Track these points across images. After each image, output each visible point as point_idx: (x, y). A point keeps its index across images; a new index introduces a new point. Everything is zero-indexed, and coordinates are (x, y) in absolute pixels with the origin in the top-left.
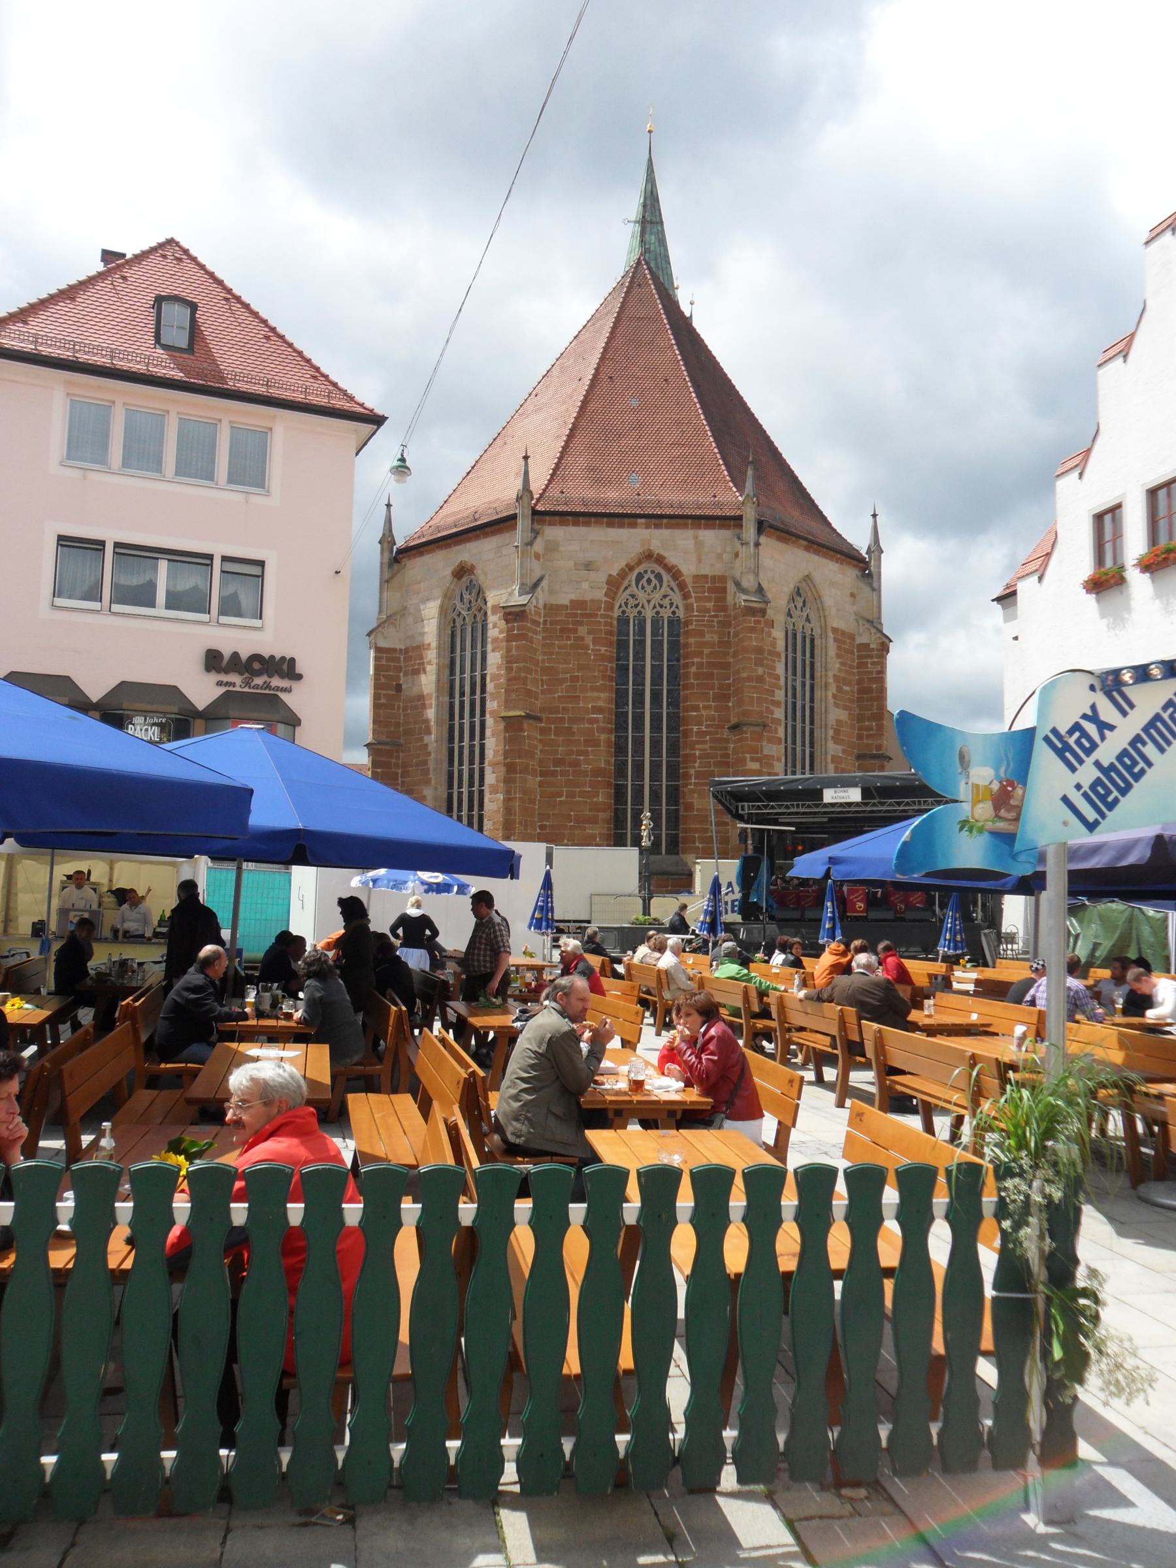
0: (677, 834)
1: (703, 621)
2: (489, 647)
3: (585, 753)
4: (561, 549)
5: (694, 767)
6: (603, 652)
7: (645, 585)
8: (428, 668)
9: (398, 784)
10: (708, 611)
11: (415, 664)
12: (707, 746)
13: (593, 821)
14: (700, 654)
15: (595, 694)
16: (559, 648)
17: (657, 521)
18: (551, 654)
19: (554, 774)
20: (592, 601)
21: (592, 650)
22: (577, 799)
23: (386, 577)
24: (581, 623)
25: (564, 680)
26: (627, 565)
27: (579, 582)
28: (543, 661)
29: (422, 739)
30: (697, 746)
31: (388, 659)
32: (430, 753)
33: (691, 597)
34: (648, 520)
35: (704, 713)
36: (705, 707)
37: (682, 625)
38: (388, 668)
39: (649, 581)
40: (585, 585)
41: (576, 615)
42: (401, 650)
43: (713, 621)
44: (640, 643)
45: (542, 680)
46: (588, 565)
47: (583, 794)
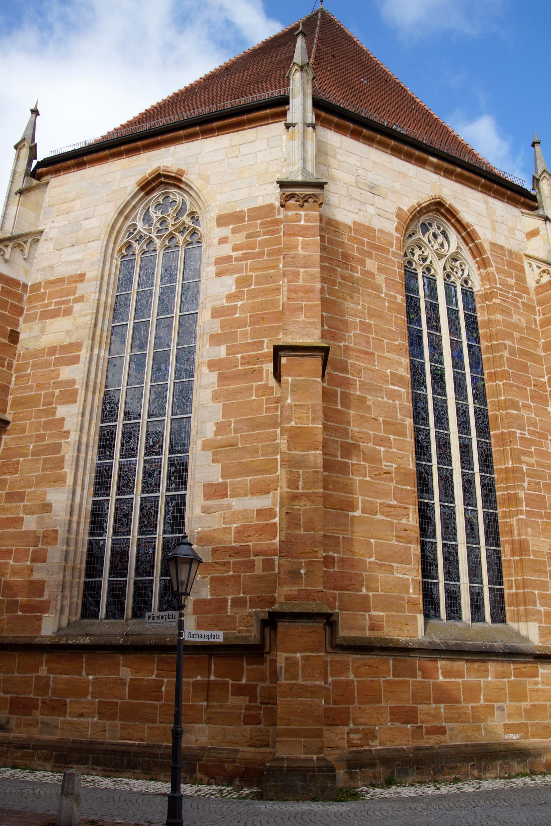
0: (502, 590)
1: (508, 298)
5: (524, 489)
7: (431, 237)
8: (77, 307)
10: (510, 287)
12: (533, 460)
14: (510, 337)
16: (343, 277)
17: (451, 167)
20: (380, 231)
21: (386, 295)
22: (379, 517)
23: (19, 185)
24: (370, 256)
29: (53, 412)
30: (524, 458)
32: (68, 432)
33: (491, 265)
34: (441, 162)
36: (525, 406)
37: (477, 299)
39: (435, 236)
41: (362, 243)
44: (433, 308)
46: (373, 187)
47: (387, 509)
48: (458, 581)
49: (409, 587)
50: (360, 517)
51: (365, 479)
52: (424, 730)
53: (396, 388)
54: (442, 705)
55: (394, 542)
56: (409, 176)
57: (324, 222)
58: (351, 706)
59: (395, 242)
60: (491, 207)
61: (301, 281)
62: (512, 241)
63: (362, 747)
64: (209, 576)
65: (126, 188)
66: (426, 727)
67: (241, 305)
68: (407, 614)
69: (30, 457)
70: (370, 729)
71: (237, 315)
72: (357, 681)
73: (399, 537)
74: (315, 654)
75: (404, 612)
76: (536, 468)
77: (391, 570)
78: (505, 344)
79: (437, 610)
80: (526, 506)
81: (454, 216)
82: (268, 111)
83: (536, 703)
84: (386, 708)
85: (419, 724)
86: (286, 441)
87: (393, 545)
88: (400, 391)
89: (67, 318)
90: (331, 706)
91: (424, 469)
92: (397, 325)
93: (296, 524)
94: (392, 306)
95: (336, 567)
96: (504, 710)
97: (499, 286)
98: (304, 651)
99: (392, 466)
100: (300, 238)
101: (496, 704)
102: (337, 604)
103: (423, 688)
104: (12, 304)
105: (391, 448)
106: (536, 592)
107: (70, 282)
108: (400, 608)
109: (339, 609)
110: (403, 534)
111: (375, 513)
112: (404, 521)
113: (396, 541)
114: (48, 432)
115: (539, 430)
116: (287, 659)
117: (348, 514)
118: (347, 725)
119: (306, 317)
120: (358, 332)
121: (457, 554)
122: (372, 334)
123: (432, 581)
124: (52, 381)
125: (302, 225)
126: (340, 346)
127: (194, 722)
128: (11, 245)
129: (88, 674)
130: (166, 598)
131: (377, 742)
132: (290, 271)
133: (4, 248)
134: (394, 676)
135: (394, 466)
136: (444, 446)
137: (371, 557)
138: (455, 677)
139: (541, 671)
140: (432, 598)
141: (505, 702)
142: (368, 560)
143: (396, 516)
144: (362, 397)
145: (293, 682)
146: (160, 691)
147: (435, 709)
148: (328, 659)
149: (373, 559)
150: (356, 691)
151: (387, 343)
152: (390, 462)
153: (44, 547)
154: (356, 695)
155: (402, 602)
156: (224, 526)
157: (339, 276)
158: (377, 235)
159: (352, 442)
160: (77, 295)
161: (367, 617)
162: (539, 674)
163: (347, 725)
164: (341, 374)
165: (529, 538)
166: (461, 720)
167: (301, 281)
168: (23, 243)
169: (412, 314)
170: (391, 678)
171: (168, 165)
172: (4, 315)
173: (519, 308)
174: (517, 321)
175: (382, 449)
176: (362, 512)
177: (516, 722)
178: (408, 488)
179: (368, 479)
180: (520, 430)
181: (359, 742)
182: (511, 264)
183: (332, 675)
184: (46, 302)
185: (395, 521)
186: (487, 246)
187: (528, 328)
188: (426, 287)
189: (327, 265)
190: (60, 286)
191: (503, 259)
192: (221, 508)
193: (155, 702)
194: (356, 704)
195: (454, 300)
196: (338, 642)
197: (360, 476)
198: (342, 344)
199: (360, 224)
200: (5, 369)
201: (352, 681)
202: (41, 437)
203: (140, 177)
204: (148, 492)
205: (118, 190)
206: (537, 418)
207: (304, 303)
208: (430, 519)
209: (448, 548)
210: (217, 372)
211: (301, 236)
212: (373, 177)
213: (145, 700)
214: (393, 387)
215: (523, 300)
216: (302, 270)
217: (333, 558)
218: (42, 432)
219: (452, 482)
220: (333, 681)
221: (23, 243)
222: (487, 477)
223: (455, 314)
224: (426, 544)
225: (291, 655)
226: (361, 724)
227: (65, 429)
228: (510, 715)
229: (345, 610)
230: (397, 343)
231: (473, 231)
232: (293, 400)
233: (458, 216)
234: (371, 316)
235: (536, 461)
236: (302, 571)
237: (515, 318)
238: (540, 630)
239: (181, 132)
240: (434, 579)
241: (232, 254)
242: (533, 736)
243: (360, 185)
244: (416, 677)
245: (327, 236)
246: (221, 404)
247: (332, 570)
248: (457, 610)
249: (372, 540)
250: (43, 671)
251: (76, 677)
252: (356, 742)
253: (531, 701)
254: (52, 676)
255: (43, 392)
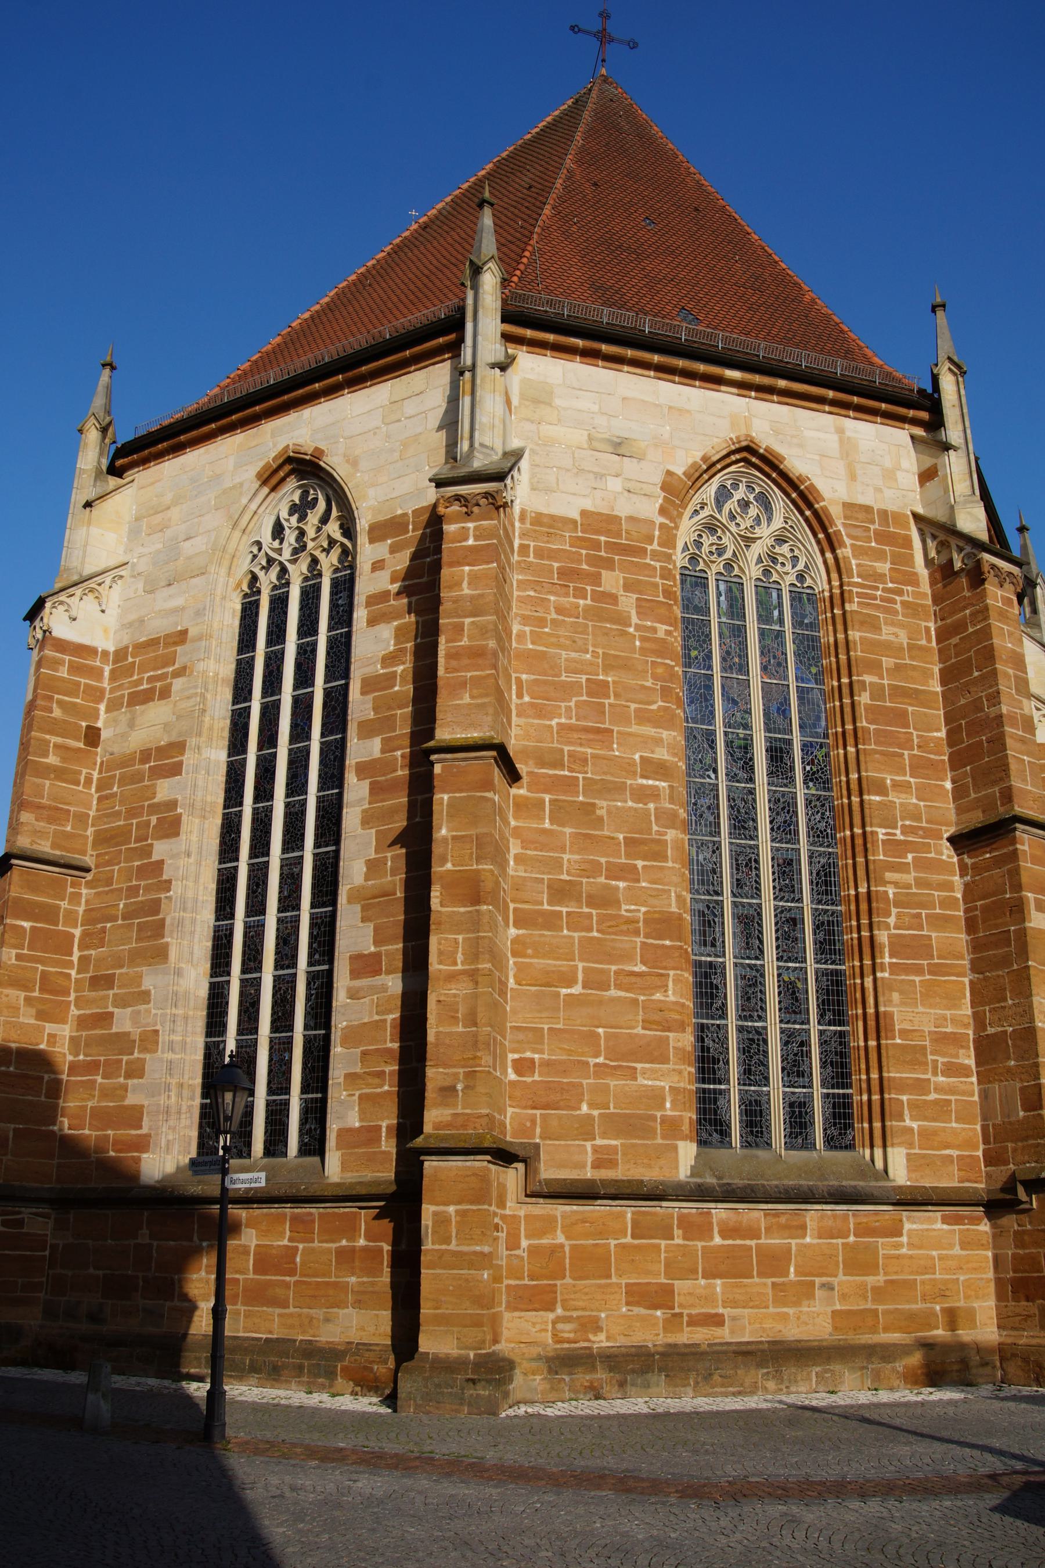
1: (876, 599)
2: (360, 614)
3: (628, 873)
4: (557, 402)
5: (887, 927)
6: (661, 634)
9: (70, 964)
10: (880, 577)
11: (139, 682)
12: (909, 878)
13: (656, 1053)
14: (875, 667)
15: (649, 731)
16: (559, 610)
18: (541, 622)
19: (551, 921)
20: (631, 519)
21: (638, 627)
24: (609, 564)
25: (568, 690)
26: (704, 459)
27: (600, 476)
28: (521, 636)
29: (147, 851)
30: (889, 876)
31: (74, 669)
35: (892, 797)
38: (73, 689)
40: (615, 485)
41: (596, 545)
42: (105, 653)
43: (894, 602)
45: (519, 681)
46: (620, 444)
47: (628, 980)
48: (767, 1085)
49: (663, 1100)
50: (580, 994)
51: (590, 935)
52: (685, 1319)
53: (650, 782)
54: (719, 1282)
55: (639, 1030)
56: (688, 411)
57: (528, 521)
58: (558, 1283)
59: (657, 533)
60: (849, 438)
61: (466, 639)
62: (888, 493)
63: (576, 1342)
64: (357, 1093)
65: (241, 484)
66: (689, 1315)
67: (403, 671)
68: (659, 1141)
69: (120, 922)
70: (590, 1316)
71: (397, 688)
72: (570, 1245)
73: (650, 1022)
74: (474, 1207)
75: (655, 1138)
76: (914, 890)
77: (633, 1074)
78: (864, 682)
79: (724, 1132)
80: (891, 956)
81: (775, 467)
82: (441, 340)
83: (894, 1277)
84: (619, 1285)
85: (677, 1310)
86: (438, 894)
87: (636, 1035)
88: (657, 787)
89: (163, 702)
90: (526, 1282)
91: (708, 907)
92: (655, 677)
93: (453, 1017)
94: (647, 645)
95: (536, 1074)
96: (833, 1289)
97: (856, 580)
98: (459, 1203)
99: (639, 911)
100: (467, 568)
101: (818, 1280)
102: (538, 1130)
103: (684, 1255)
104: (86, 685)
105: (638, 881)
106: (904, 1098)
107: (167, 645)
108: (650, 1133)
109: (541, 1137)
110: (656, 1017)
111: (608, 989)
112: (658, 996)
113: (643, 1028)
114: (142, 883)
115: (924, 825)
116: (435, 1214)
117: (558, 994)
118: (552, 1309)
119: (472, 697)
120: (585, 698)
121: (765, 1041)
122: (609, 698)
123: (718, 1087)
124: (146, 804)
125: (470, 547)
126: (551, 726)
127: (338, 1307)
128: (78, 591)
129: (201, 1240)
130: (308, 1126)
131: (602, 1336)
132: (450, 624)
133: (68, 600)
134: (633, 1237)
135: (643, 909)
136: (747, 865)
137: (597, 1056)
138: (743, 1237)
139: (907, 1226)
140: (716, 1114)
141: (836, 1276)
142: (592, 1061)
143: (643, 990)
144: (588, 804)
145: (444, 1247)
146: (294, 1263)
147: (705, 1287)
148: (522, 1213)
149: (601, 1060)
150: (567, 1261)
151: (636, 710)
152: (636, 904)
153: (141, 1056)
154: (567, 1266)
155: (651, 1124)
156: (377, 1018)
157: (552, 609)
158: (624, 527)
159: (568, 878)
160: (177, 666)
161: (589, 1149)
162: (905, 1232)
163: (552, 1309)
164: (551, 772)
165: (895, 1009)
166: (751, 1304)
167: (466, 639)
168: (97, 587)
169: (695, 649)
170: (628, 1240)
171: (300, 441)
172: (75, 704)
173: (895, 612)
174: (892, 638)
175: (622, 884)
176: (584, 987)
177: (855, 1308)
178: (667, 943)
179: (595, 934)
180: (885, 827)
181: (572, 1335)
182: (883, 537)
183: (527, 1237)
184: (135, 677)
185: (642, 998)
186: (836, 512)
187: (911, 647)
188: (722, 598)
189: (532, 593)
190: (154, 651)
191: (868, 529)
192: (373, 990)
193: (288, 1278)
194: (568, 1280)
195: (776, 613)
196: (537, 1188)
197: (582, 931)
198: (554, 722)
199: (593, 513)
200: (80, 788)
201: (562, 1246)
202: (133, 891)
203: (261, 464)
204: (282, 968)
205: (231, 489)
206: (922, 803)
207: (469, 674)
208: (717, 988)
209: (749, 1032)
210: (368, 781)
211: (469, 565)
212: (621, 427)
213: (275, 1275)
214: (644, 782)
215: (906, 598)
216: (468, 621)
217: (532, 1060)
218: (134, 883)
219: (760, 925)
220: (530, 1245)
221: (97, 587)
222: (828, 910)
223: (777, 637)
224: (708, 1028)
225: (441, 1208)
226: (576, 1309)
227: (165, 877)
228: (843, 1297)
229: (550, 1139)
230: (654, 707)
231: (812, 488)
232: (449, 830)
233: (782, 467)
234: (607, 668)
235: (915, 879)
236: (459, 1087)
237: (887, 634)
238: (908, 1160)
239: (317, 385)
240: (720, 1083)
241: (390, 587)
242: (886, 1330)
243: (596, 444)
244: (673, 1239)
245: (532, 544)
246: (373, 831)
247: (529, 1080)
248: (762, 1133)
249: (600, 1030)
250: (144, 1237)
251: (185, 1243)
252: (566, 1335)
253: (885, 1274)
254: (155, 1243)
255: (134, 821)
